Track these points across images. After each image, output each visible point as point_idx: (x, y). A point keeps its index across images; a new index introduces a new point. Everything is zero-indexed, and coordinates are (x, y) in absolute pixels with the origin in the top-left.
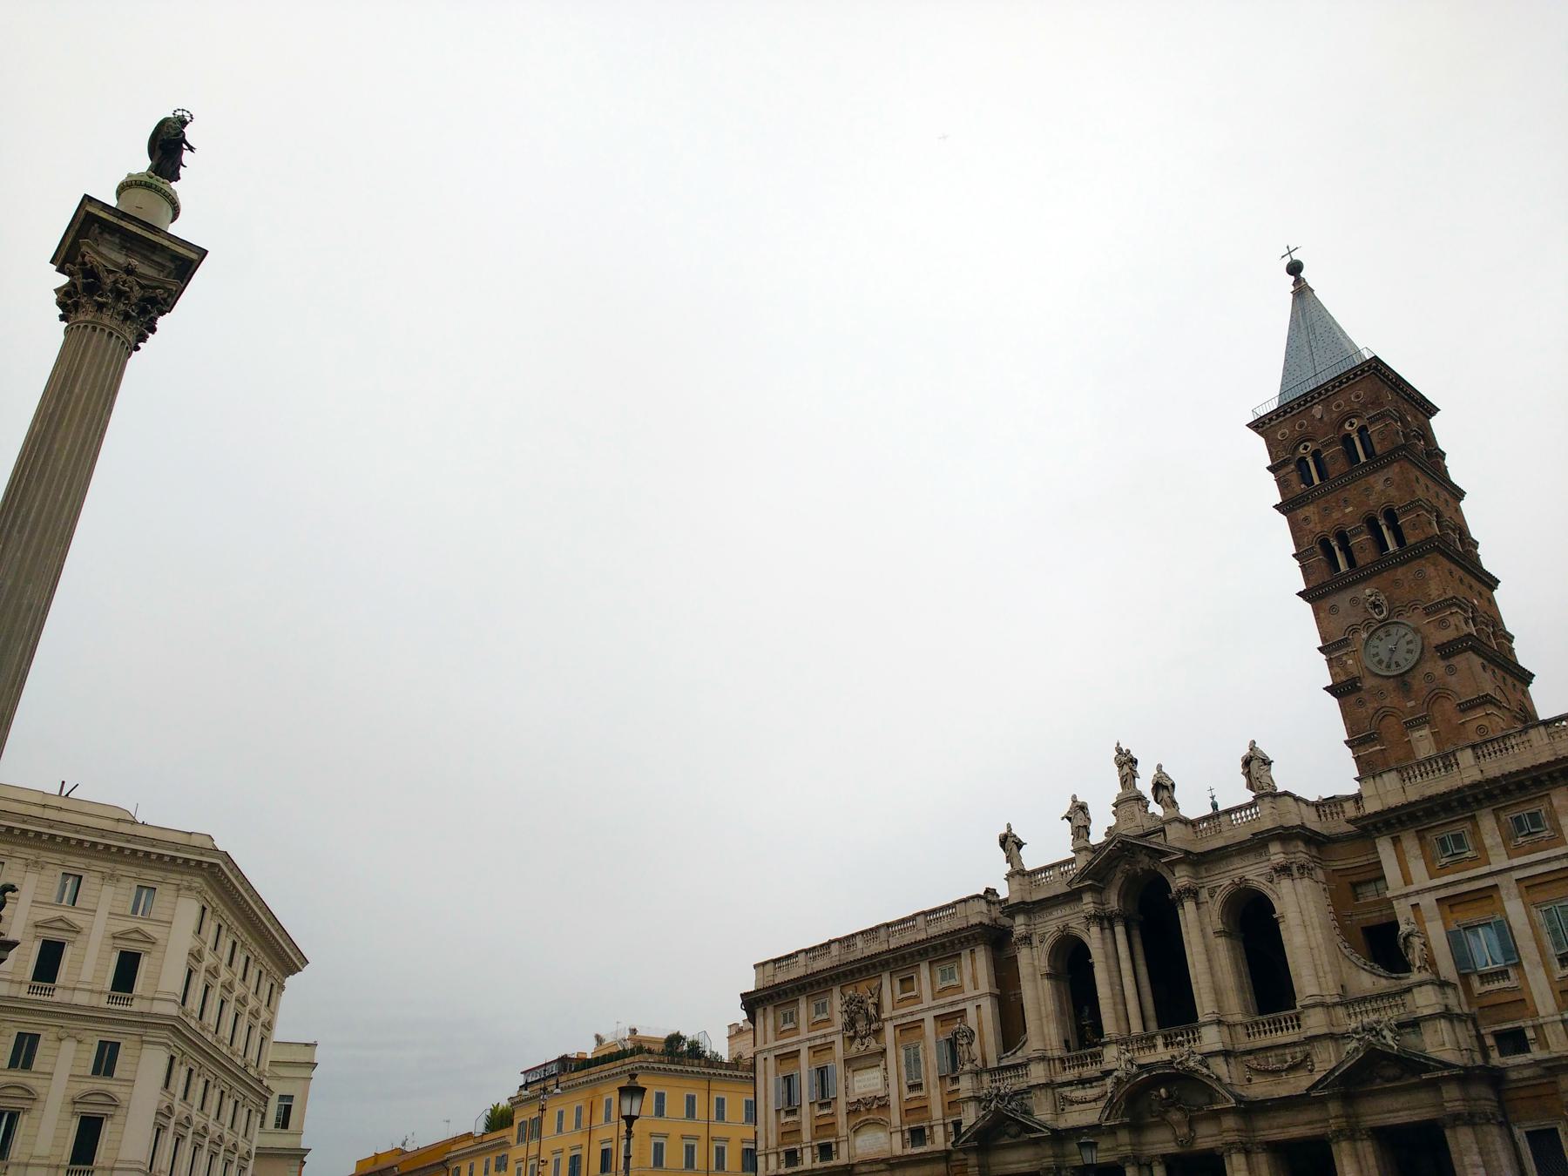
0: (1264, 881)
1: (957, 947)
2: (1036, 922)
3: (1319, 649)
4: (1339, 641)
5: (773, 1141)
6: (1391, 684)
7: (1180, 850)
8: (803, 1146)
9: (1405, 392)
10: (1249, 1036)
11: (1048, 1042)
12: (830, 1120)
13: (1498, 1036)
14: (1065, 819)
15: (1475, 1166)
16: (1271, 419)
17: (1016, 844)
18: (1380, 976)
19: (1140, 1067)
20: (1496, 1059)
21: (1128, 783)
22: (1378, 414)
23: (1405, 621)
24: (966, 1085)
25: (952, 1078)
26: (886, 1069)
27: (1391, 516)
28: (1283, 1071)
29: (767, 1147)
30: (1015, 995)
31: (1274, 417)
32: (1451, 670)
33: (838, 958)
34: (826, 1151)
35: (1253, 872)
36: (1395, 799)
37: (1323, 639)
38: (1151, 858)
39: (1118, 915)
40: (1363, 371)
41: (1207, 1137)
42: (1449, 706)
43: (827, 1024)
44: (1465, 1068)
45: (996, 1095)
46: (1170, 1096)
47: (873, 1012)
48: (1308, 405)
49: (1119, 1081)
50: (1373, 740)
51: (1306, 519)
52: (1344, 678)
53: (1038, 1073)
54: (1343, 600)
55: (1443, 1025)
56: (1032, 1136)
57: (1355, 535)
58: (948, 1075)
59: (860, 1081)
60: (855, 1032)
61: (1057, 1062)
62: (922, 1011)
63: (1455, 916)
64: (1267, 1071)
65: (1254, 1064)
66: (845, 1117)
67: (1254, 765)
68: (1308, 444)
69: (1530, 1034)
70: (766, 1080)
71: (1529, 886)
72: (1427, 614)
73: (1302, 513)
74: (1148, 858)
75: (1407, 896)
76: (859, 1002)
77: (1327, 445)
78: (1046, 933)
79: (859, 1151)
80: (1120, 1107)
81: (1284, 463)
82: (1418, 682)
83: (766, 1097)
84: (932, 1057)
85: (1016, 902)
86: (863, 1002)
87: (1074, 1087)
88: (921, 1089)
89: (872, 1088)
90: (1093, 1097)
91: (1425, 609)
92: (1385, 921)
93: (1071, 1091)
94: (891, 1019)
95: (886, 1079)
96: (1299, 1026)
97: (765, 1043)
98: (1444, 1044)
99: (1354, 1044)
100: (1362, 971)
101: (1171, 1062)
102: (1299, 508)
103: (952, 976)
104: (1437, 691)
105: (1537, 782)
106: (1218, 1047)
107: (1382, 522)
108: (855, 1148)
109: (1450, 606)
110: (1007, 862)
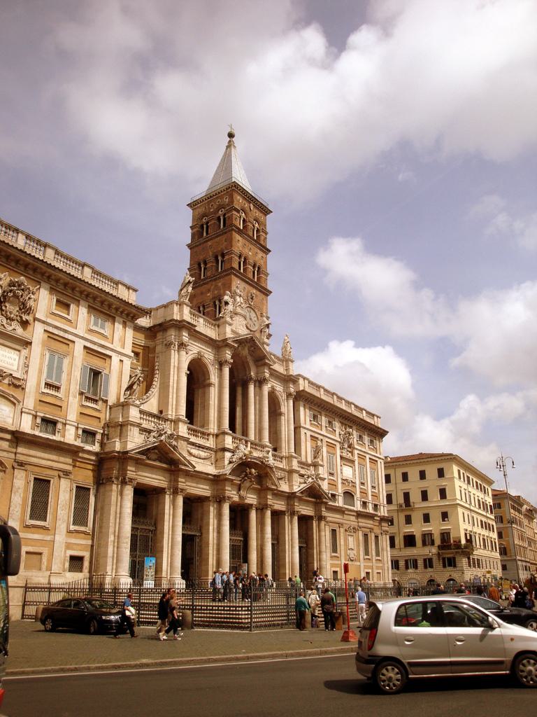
25: (87, 398)
27: (259, 268)
41: (251, 499)
49: (241, 458)
62: (76, 335)
73: (237, 237)
75: (305, 428)
76: (23, 290)
81: (238, 211)
84: (77, 374)
94: (44, 322)
103: (103, 327)
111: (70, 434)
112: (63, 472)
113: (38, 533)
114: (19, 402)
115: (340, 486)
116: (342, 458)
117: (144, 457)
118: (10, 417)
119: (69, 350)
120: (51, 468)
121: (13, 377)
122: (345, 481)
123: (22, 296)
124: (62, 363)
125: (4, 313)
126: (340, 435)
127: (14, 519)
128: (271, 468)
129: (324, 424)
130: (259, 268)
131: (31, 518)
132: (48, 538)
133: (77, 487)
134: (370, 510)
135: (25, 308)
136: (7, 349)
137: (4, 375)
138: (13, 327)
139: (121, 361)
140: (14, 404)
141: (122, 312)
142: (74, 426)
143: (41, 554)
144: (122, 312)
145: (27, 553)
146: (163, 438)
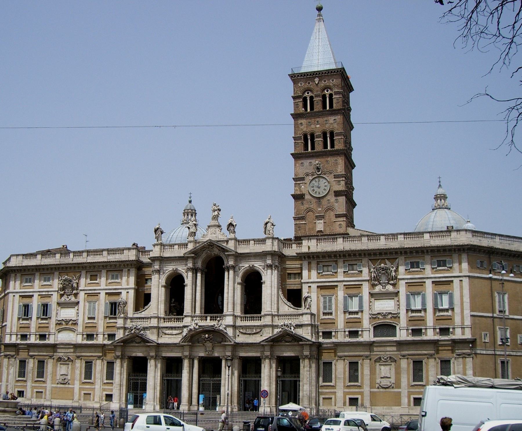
0: (261, 268)
1: (121, 267)
2: (163, 265)
3: (293, 179)
4: (300, 178)
5: (14, 330)
6: (314, 200)
8: (31, 333)
9: (347, 82)
10: (241, 320)
11: (159, 311)
12: (47, 325)
14: (187, 228)
15: (307, 371)
16: (298, 76)
17: (161, 232)
18: (291, 307)
19: (199, 326)
20: (321, 340)
21: (215, 218)
22: (338, 92)
23: (326, 178)
24: (120, 322)
26: (78, 310)
28: (251, 334)
29: (11, 331)
30: (142, 289)
31: (300, 76)
33: (59, 260)
34: (43, 337)
35: (258, 265)
36: (313, 249)
37: (295, 175)
38: (219, 250)
39: (200, 269)
40: (338, 71)
42: (332, 214)
43: (50, 287)
44: (313, 342)
45: (135, 328)
46: (209, 338)
47: (76, 286)
48: (314, 76)
49: (191, 330)
50: (303, 219)
51: (301, 124)
52: (299, 193)
53: (154, 322)
55: (310, 328)
56: (149, 344)
57: (317, 137)
58: (108, 316)
59: (64, 312)
60: (64, 292)
61: (162, 320)
63: (322, 292)
64: (245, 334)
65: (241, 331)
66: (54, 325)
67: (269, 225)
68: (309, 92)
70: (13, 304)
71: (347, 287)
72: (335, 178)
73: (300, 121)
74: (218, 250)
75: (308, 283)
76: (69, 281)
77: (317, 96)
78: (167, 270)
79: (59, 339)
80: (188, 338)
82: (324, 202)
83: (13, 311)
85: (157, 256)
86: (71, 281)
89: (69, 316)
90: (175, 333)
91: (334, 175)
92: (295, 288)
93: (166, 330)
94: (84, 290)
95: (77, 313)
96: (260, 320)
97: (15, 289)
98: (309, 334)
99: (281, 329)
100: (285, 304)
101: (212, 326)
102: (300, 118)
104: (330, 207)
105: (360, 255)
106: (232, 323)
107: (328, 135)
108: (58, 338)
109: (343, 177)
110: (156, 238)
111: (100, 339)
112: (97, 357)
113: (88, 385)
114: (76, 330)
117: (122, 344)
118: (73, 338)
119: (98, 298)
120: (92, 356)
121: (73, 320)
122: (373, 317)
123: (70, 283)
124: (95, 306)
127: (77, 380)
130: (332, 134)
131: (85, 379)
132: (93, 387)
133: (107, 362)
134: (430, 335)
135: (73, 289)
136: (70, 309)
139: (128, 292)
140: (74, 332)
141: (124, 265)
142: (102, 334)
143: (90, 394)
145: (85, 394)
146: (133, 332)
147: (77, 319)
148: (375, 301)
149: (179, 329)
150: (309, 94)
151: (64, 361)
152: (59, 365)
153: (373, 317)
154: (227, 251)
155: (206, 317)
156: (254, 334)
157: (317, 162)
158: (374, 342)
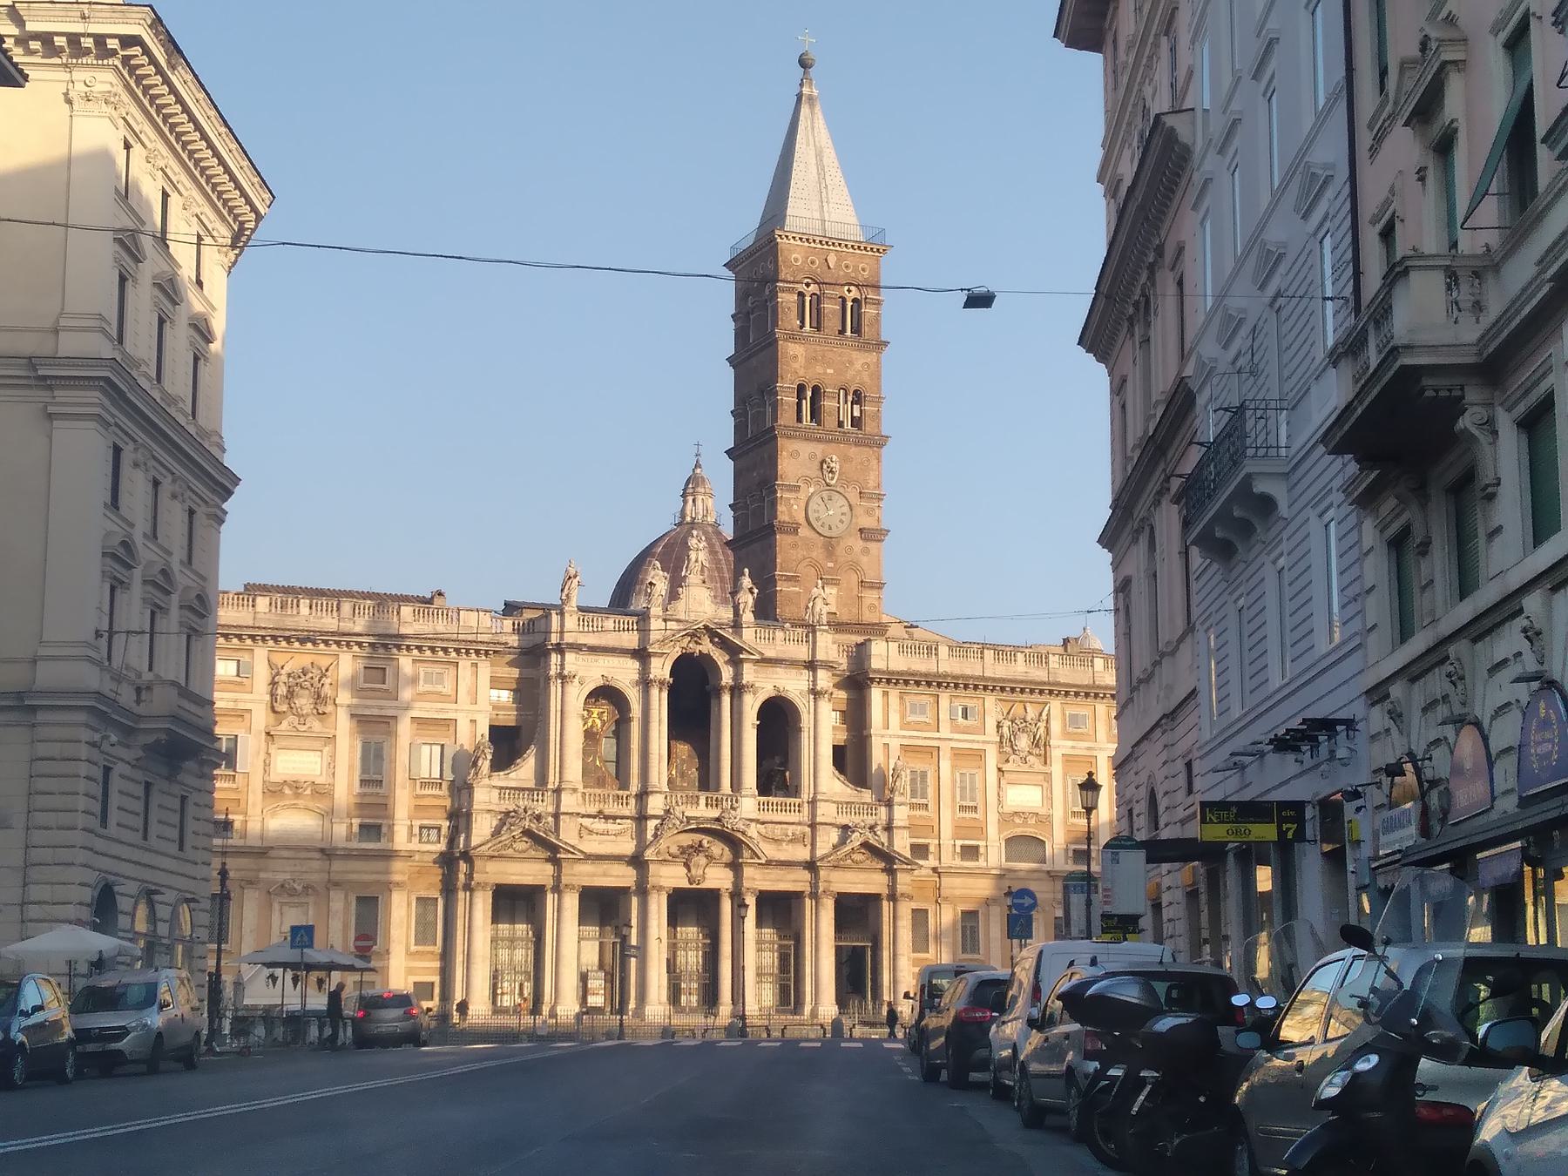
7: (760, 653)
13: (914, 848)
26: (333, 756)
32: (866, 551)
35: (793, 685)
41: (717, 878)
43: (237, 688)
52: (787, 519)
54: (806, 449)
69: (932, 849)
71: (958, 754)
75: (883, 736)
81: (791, 290)
82: (840, 551)
87: (597, 820)
88: (381, 786)
103: (440, 681)
115: (992, 830)
116: (999, 770)
120: (378, 882)
122: (1006, 819)
125: (294, 711)
126: (999, 726)
128: (743, 833)
129: (944, 715)
133: (417, 898)
135: (319, 698)
137: (305, 785)
138: (308, 725)
139: (473, 721)
144: (467, 652)
147: (331, 781)
148: (1009, 786)
149: (624, 821)
150: (810, 288)
151: (292, 895)
152: (276, 906)
153: (1006, 819)
154: (741, 650)
155: (698, 797)
156: (791, 841)
157: (835, 458)
158: (1010, 870)
